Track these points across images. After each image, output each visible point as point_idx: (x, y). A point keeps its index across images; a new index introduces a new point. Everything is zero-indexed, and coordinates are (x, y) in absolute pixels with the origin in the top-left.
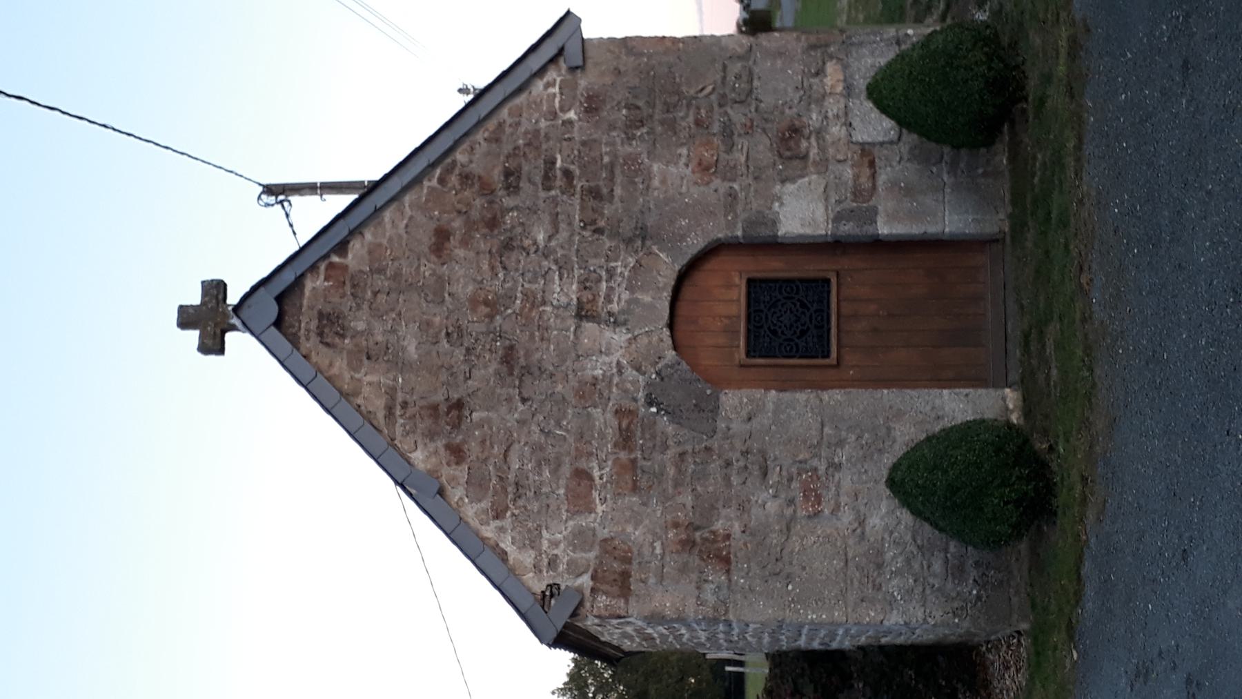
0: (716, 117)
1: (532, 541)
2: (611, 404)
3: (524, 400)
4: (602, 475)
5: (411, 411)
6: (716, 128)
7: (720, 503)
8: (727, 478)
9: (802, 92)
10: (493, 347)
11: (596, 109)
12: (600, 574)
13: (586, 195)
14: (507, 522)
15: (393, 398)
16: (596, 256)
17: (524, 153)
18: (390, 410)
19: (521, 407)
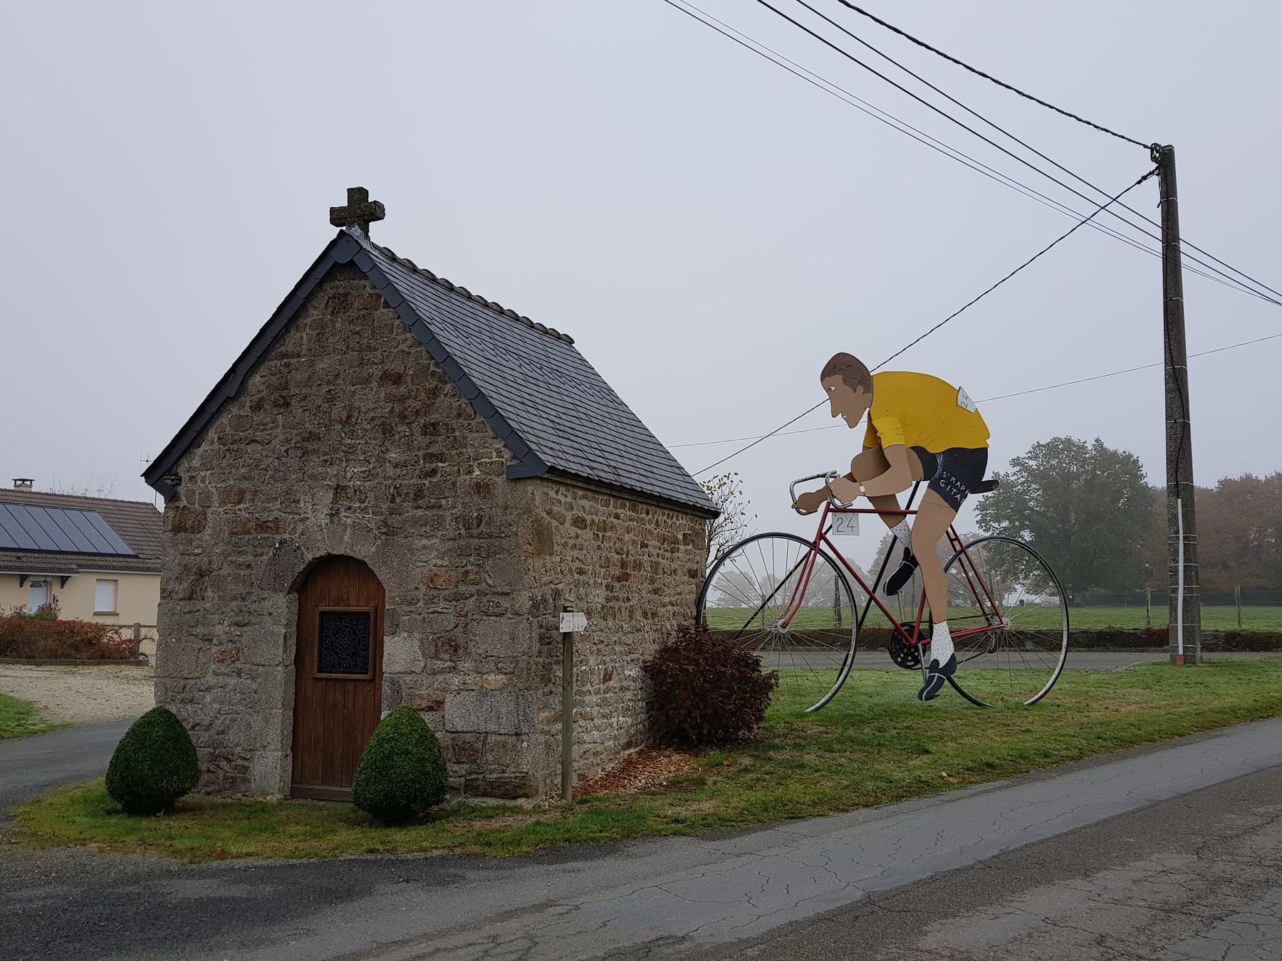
0: (470, 588)
1: (206, 465)
2: (282, 514)
3: (287, 451)
4: (241, 511)
5: (284, 370)
6: (462, 588)
7: (221, 593)
8: (234, 598)
9: (484, 656)
10: (322, 426)
11: (479, 492)
12: (186, 512)
13: (418, 488)
14: (216, 446)
15: (292, 356)
16: (376, 498)
17: (449, 437)
18: (284, 356)
19: (283, 449)
